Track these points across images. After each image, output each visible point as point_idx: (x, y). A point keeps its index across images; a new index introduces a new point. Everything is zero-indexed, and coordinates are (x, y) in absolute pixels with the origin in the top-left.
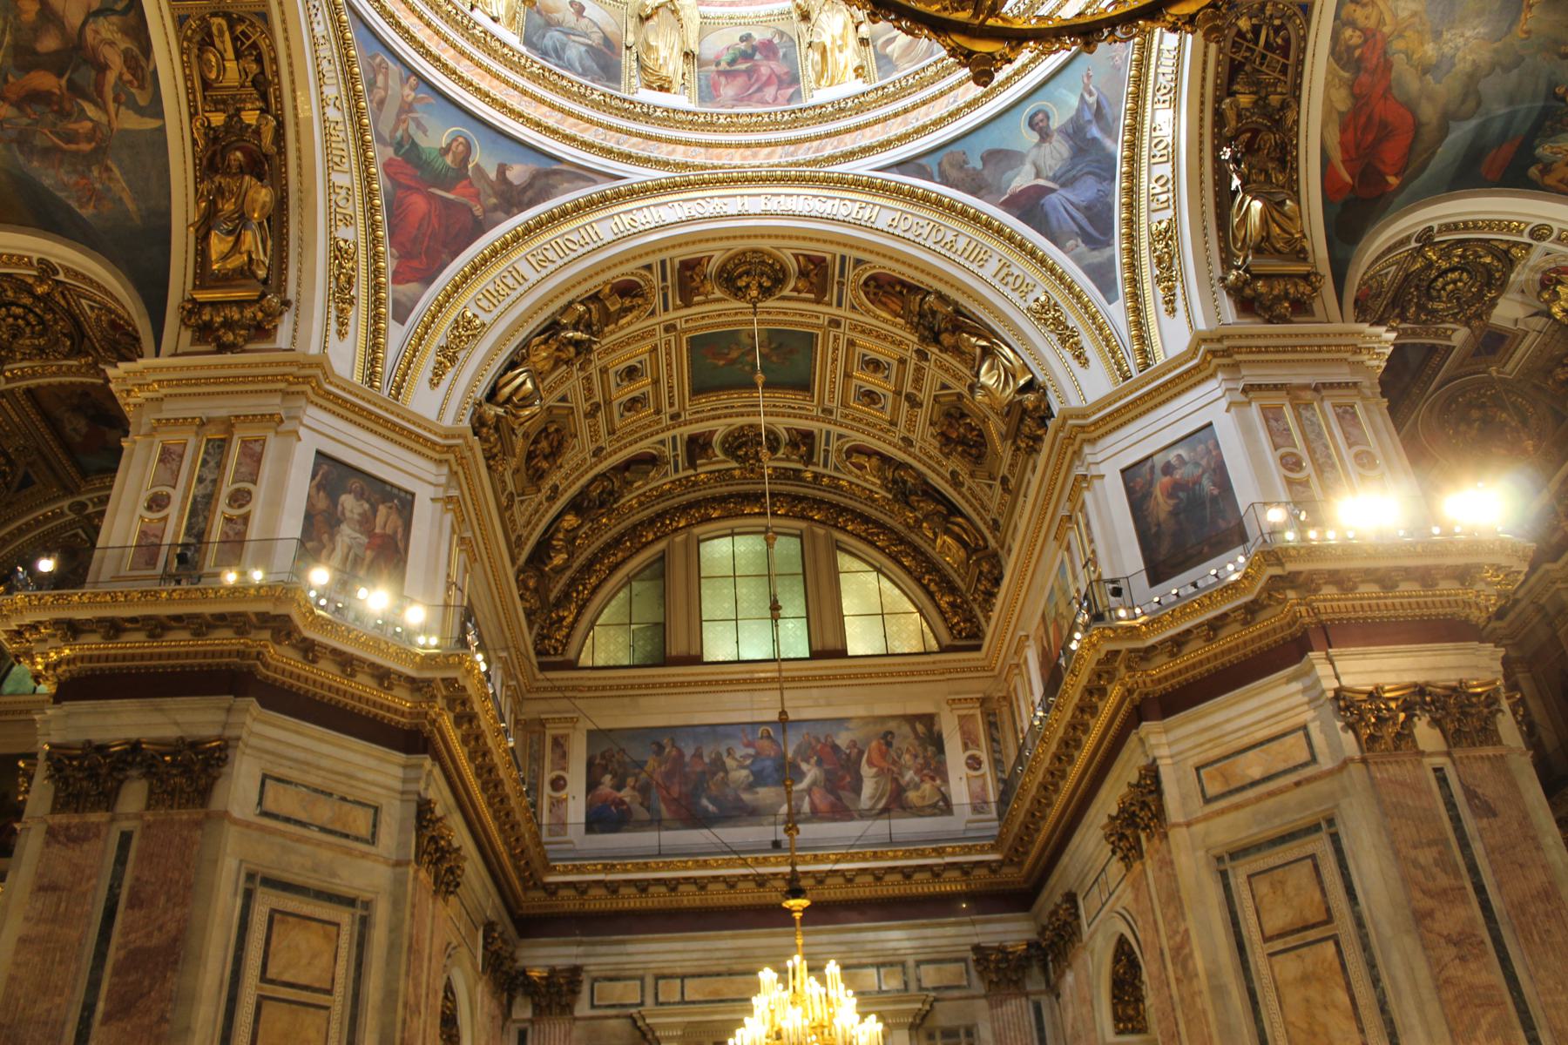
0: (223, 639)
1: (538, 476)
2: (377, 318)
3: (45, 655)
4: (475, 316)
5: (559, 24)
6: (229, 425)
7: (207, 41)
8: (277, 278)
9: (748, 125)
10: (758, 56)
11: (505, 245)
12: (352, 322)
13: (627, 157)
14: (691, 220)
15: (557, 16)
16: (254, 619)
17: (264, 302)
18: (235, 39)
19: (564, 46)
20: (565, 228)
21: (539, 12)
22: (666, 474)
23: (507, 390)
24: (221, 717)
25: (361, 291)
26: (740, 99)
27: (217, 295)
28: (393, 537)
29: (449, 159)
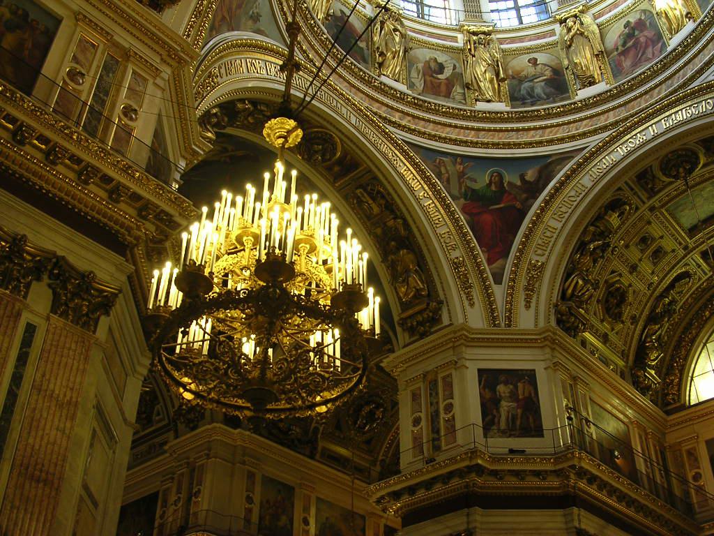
0: (455, 482)
1: (617, 317)
2: (487, 288)
3: (392, 508)
4: (538, 261)
5: (526, 77)
6: (436, 372)
7: (360, 202)
8: (432, 294)
9: (642, 80)
10: (636, 33)
11: (538, 216)
12: (475, 297)
13: (584, 135)
14: (630, 153)
15: (524, 73)
16: (465, 470)
17: (430, 307)
18: (369, 194)
19: (532, 88)
20: (566, 191)
21: (513, 78)
22: (700, 279)
23: (570, 291)
24: (465, 519)
25: (473, 279)
26: (635, 65)
27: (410, 312)
28: (530, 397)
29: (493, 188)
